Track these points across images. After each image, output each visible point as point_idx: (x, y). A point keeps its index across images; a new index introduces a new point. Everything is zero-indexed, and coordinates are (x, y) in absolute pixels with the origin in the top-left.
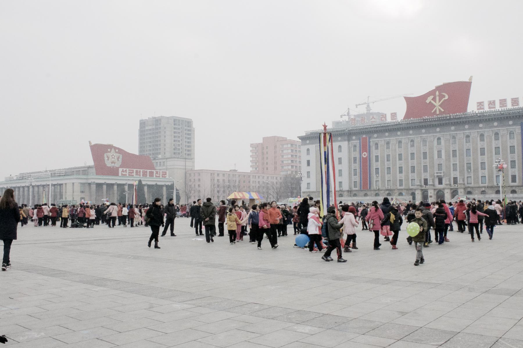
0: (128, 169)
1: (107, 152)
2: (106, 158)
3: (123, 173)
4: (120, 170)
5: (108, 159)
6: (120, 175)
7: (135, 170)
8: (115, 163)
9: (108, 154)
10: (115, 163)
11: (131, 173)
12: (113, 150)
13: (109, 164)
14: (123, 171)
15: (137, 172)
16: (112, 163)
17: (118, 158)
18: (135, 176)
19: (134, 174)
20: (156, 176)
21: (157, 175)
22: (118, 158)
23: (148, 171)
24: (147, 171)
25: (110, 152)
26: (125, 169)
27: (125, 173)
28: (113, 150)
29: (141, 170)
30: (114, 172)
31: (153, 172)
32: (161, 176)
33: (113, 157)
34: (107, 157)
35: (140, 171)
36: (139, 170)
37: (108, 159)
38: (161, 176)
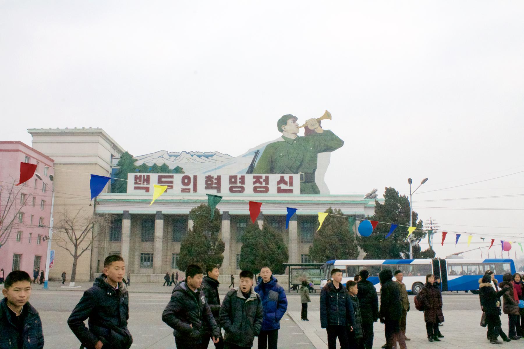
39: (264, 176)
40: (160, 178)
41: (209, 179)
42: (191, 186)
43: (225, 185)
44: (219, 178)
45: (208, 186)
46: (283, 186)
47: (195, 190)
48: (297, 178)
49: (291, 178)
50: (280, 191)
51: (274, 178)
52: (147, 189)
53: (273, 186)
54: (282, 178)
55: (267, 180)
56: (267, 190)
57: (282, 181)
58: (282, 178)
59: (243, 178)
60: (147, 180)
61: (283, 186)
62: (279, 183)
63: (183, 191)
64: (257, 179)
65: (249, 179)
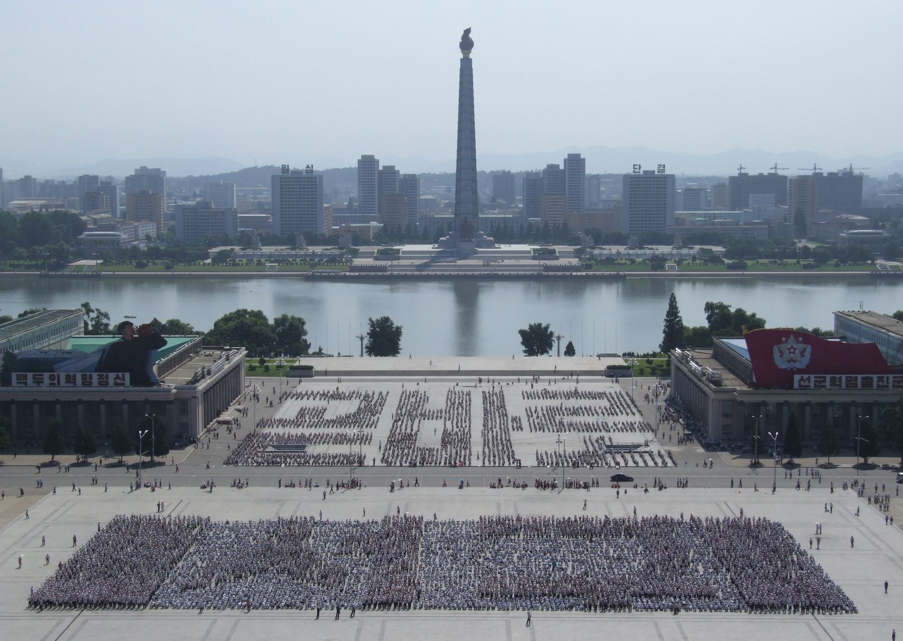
0: (812, 376)
1: (781, 342)
2: (776, 354)
3: (803, 383)
4: (797, 378)
5: (781, 356)
6: (796, 385)
7: (828, 377)
8: (794, 361)
9: (783, 347)
10: (794, 361)
11: (820, 382)
12: (792, 337)
13: (781, 363)
14: (802, 379)
15: (833, 381)
16: (789, 361)
17: (802, 355)
18: (828, 387)
19: (828, 384)
20: (878, 386)
21: (881, 383)
22: (802, 355)
23: (860, 377)
24: (856, 379)
25: (786, 342)
26: (805, 376)
27: (806, 383)
28: (792, 337)
29: (844, 377)
30: (784, 380)
31: (872, 378)
32: (891, 385)
33: (792, 350)
34: (780, 352)
35: (840, 378)
36: (838, 376)
37: (781, 356)
38: (891, 385)
39: (105, 374)
40: (34, 376)
41: (68, 376)
42: (56, 381)
43: (79, 380)
44: (74, 376)
45: (68, 381)
46: (118, 381)
47: (59, 384)
48: (127, 375)
49: (123, 376)
50: (116, 384)
51: (112, 376)
52: (26, 384)
53: (111, 381)
54: (118, 375)
55: (107, 377)
56: (107, 384)
57: (117, 377)
58: (118, 375)
59: (91, 376)
60: (26, 377)
61: (118, 381)
62: (115, 379)
63: (52, 385)
64: (101, 377)
65: (95, 376)
